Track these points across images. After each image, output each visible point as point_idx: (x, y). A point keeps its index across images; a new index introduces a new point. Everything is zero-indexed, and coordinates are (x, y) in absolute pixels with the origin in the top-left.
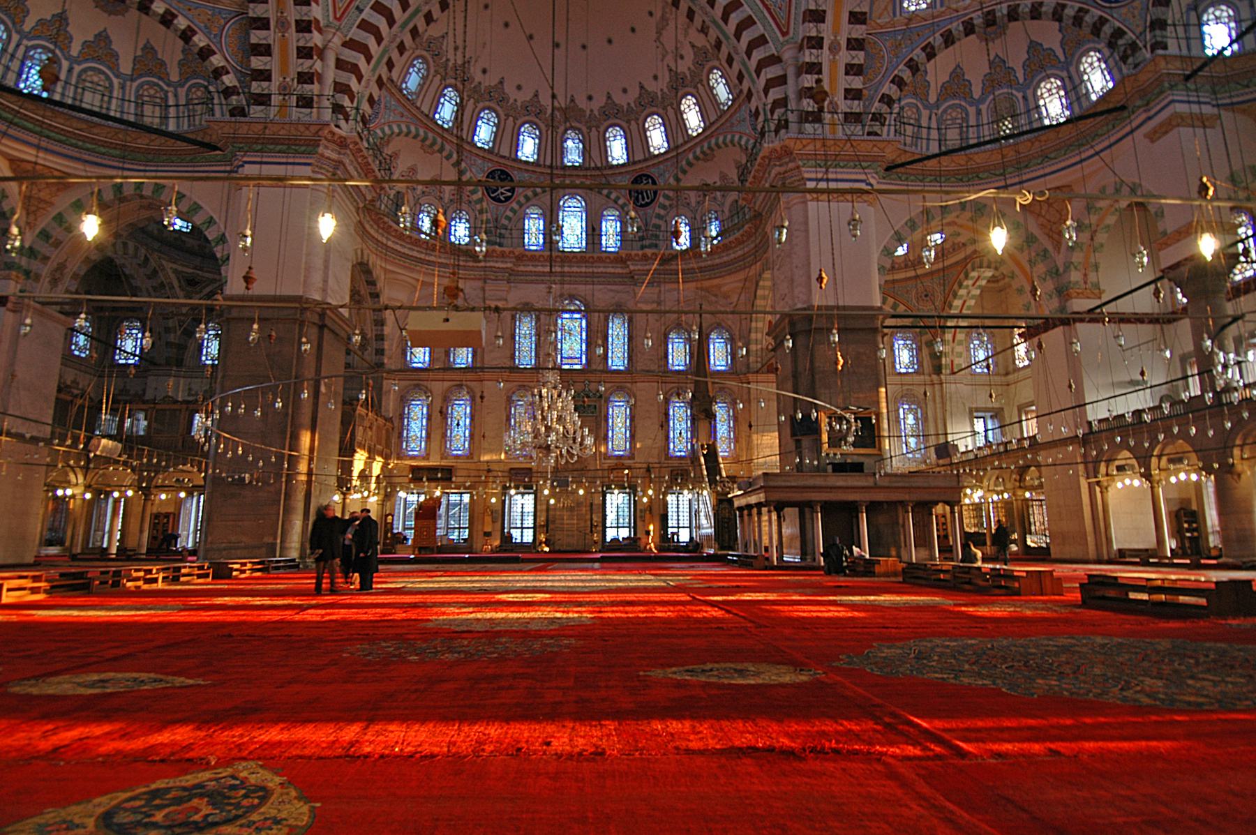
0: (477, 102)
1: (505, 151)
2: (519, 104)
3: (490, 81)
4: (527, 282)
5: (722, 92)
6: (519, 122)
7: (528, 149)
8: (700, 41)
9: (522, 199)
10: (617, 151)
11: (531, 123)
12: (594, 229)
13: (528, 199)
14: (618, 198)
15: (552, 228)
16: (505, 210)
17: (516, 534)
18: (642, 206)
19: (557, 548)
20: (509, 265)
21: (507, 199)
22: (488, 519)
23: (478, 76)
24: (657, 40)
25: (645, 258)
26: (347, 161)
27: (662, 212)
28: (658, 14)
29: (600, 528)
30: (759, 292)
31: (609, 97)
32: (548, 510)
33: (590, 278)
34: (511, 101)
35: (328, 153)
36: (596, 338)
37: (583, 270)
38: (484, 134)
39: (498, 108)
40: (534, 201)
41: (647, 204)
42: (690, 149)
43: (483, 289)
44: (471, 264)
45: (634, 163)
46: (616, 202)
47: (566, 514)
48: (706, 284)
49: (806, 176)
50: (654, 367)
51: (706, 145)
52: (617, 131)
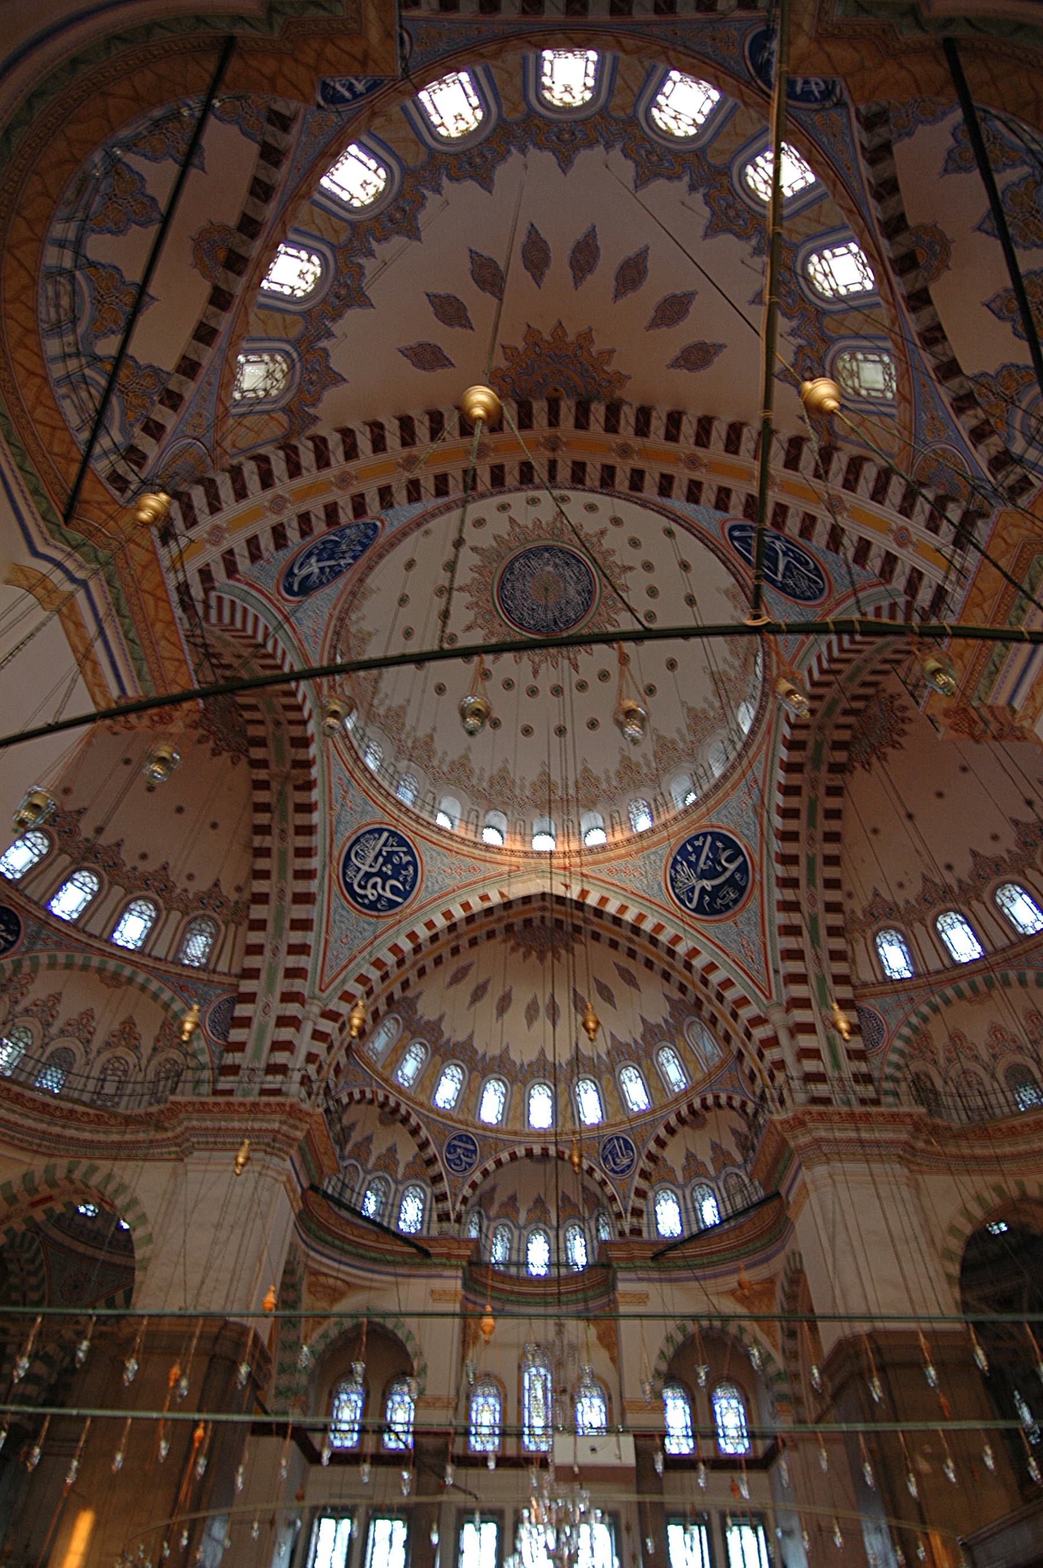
26: (817, 1134)
34: (1006, 856)
35: (803, 1140)
49: (1002, 701)
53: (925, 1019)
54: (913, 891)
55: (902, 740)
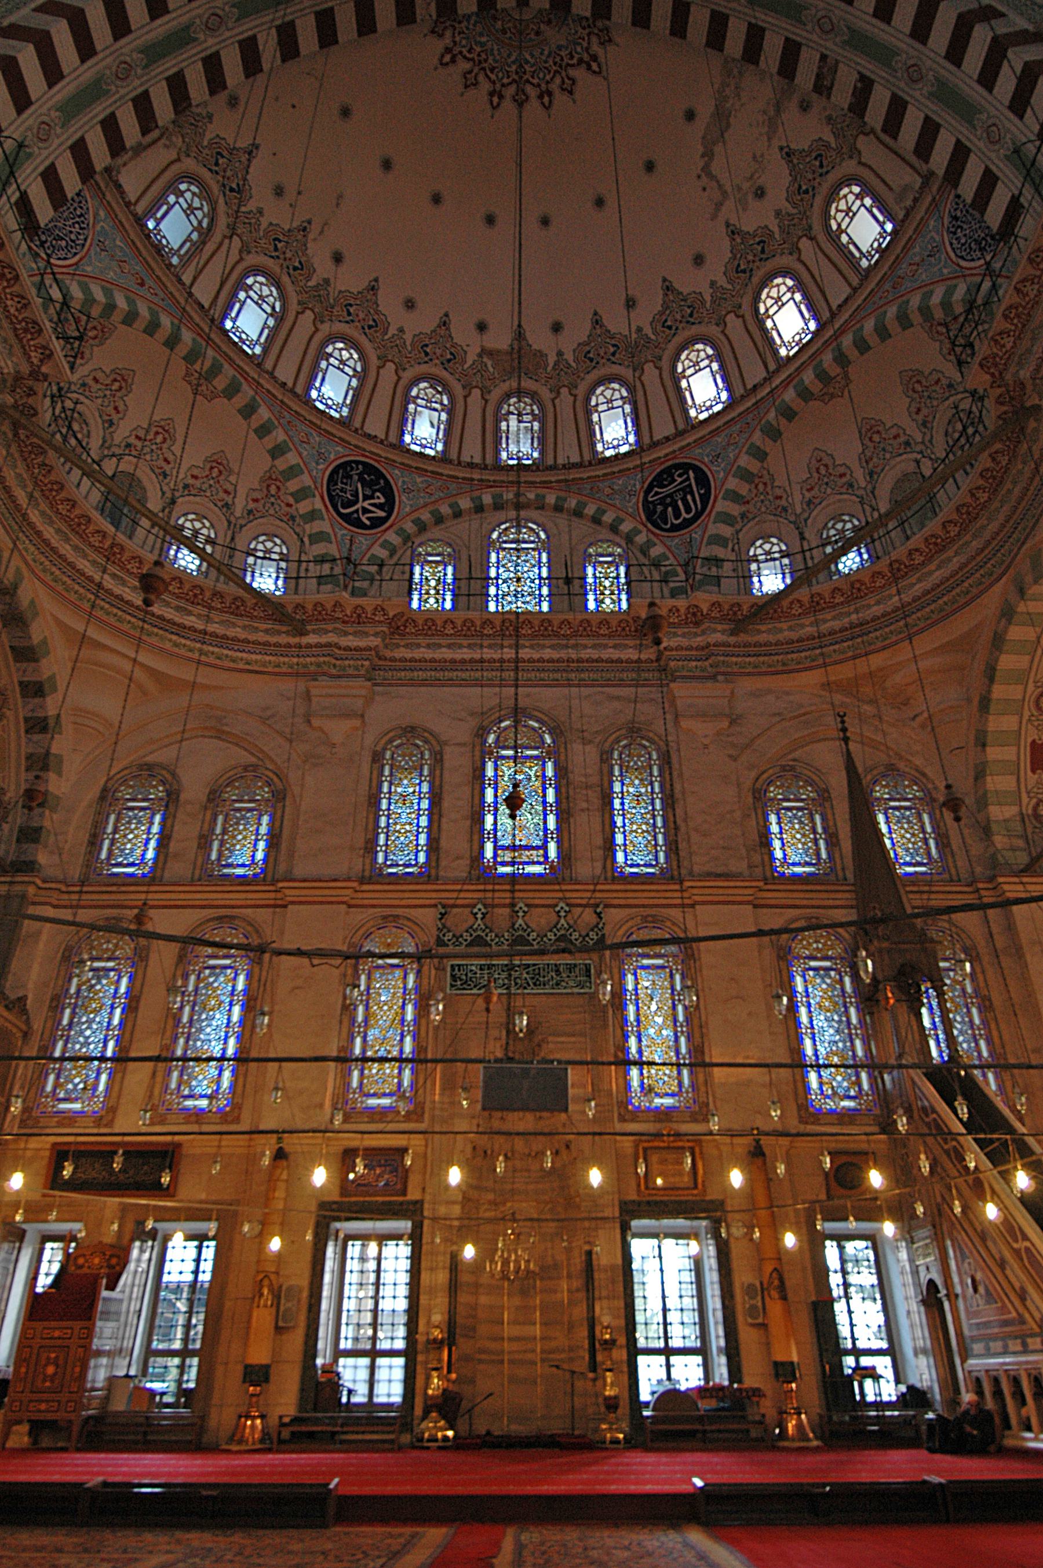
0: (318, 319)
1: (375, 426)
2: (408, 337)
3: (349, 280)
4: (412, 683)
5: (865, 230)
6: (407, 375)
7: (424, 431)
8: (806, 130)
9: (410, 527)
10: (615, 432)
11: (434, 380)
12: (568, 581)
13: (422, 527)
14: (619, 521)
15: (472, 584)
16: (371, 546)
17: (352, 1373)
18: (675, 528)
19: (481, 1427)
20: (374, 642)
21: (377, 522)
22: (263, 1317)
23: (322, 266)
24: (706, 169)
25: (695, 618)
27: (726, 531)
28: (705, 111)
29: (620, 1354)
30: (1006, 662)
31: (597, 322)
32: (453, 1287)
33: (566, 673)
34: (392, 331)
36: (582, 807)
37: (548, 653)
38: (333, 390)
39: (363, 340)
40: (436, 532)
41: (687, 523)
42: (786, 383)
43: (308, 696)
44: (283, 639)
45: (655, 445)
46: (614, 528)
47: (509, 1304)
48: (844, 672)
50: (741, 866)
51: (828, 358)
52: (617, 391)
53: (130, 318)
54: (277, 215)
55: (558, 95)
